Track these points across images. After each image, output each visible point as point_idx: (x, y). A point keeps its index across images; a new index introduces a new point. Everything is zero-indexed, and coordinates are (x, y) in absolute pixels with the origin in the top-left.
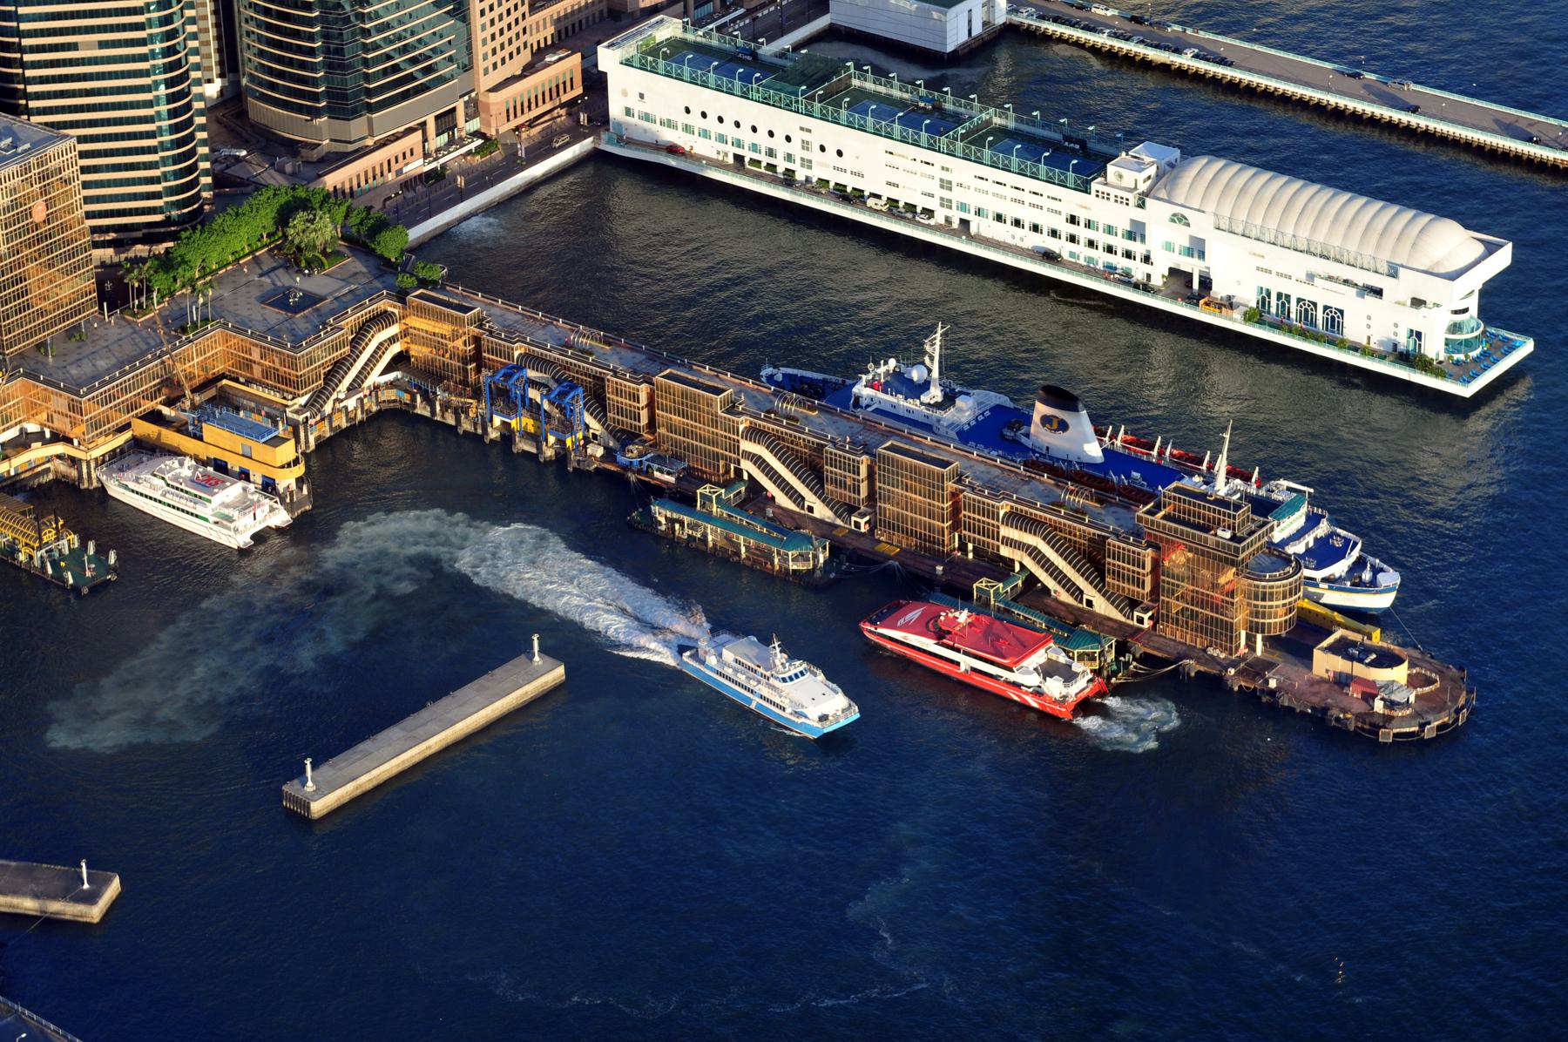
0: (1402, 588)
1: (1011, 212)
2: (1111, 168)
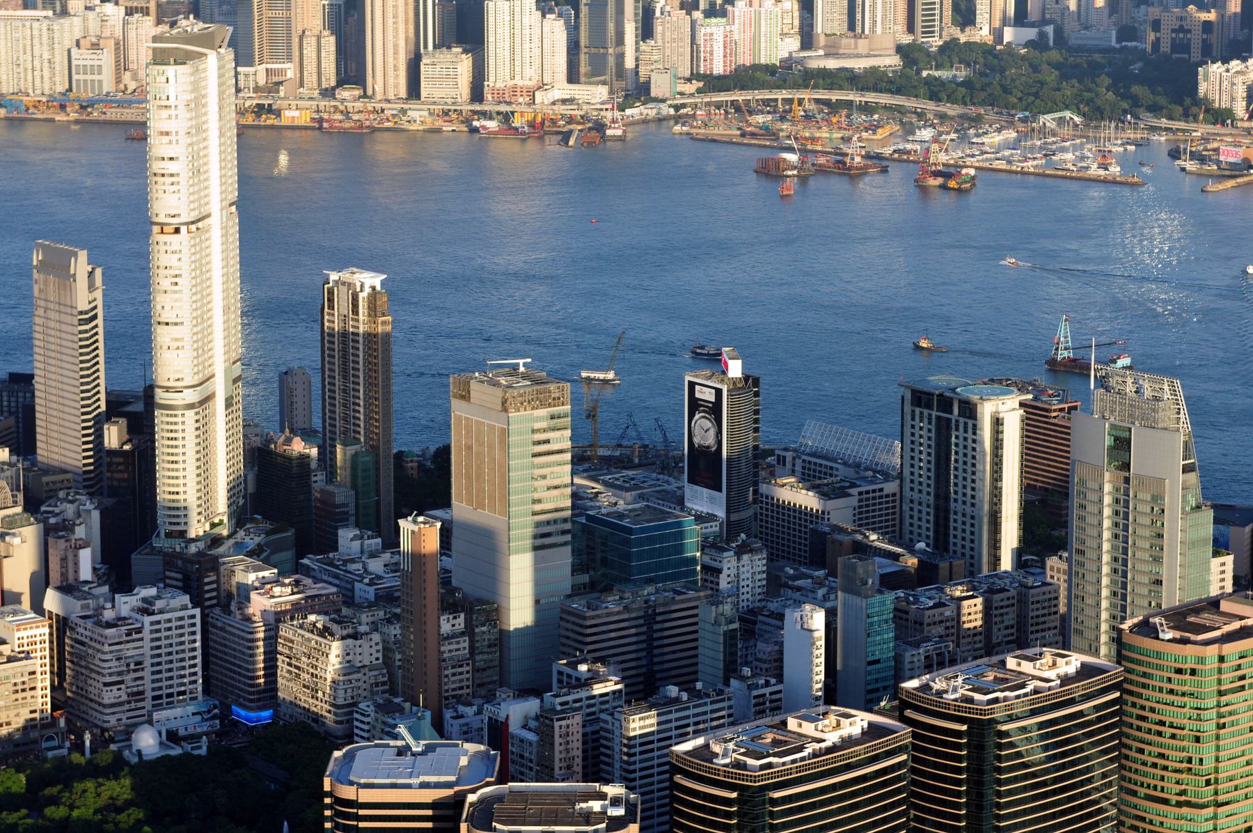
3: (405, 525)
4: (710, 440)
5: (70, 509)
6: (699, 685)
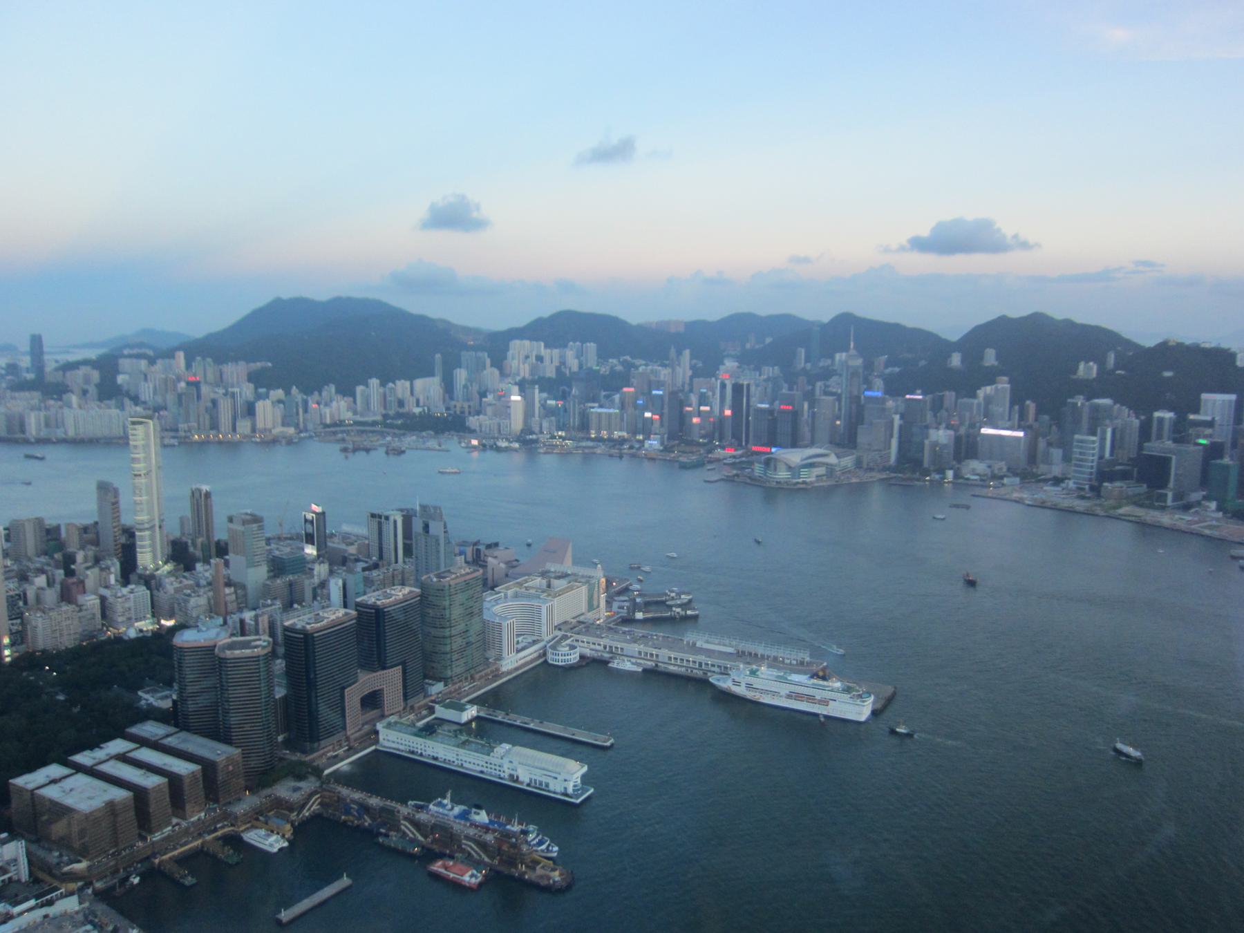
0: (559, 852)
1: (473, 761)
2: (495, 750)
3: (212, 561)
4: (309, 529)
5: (109, 562)
6: (304, 604)
